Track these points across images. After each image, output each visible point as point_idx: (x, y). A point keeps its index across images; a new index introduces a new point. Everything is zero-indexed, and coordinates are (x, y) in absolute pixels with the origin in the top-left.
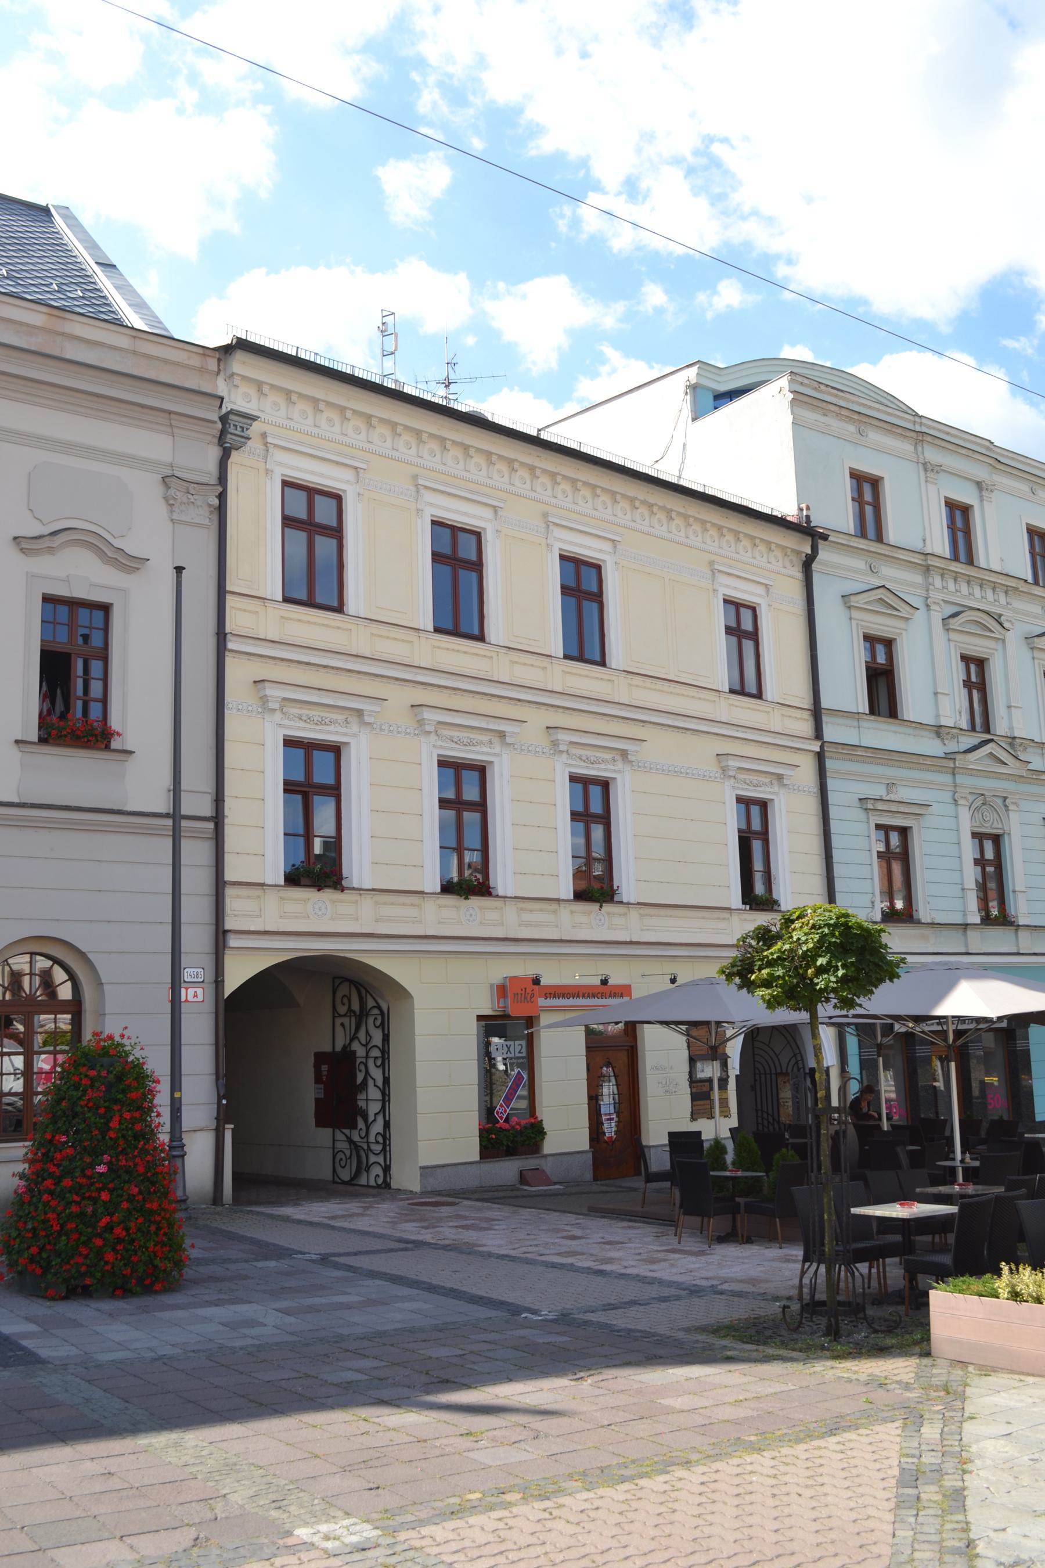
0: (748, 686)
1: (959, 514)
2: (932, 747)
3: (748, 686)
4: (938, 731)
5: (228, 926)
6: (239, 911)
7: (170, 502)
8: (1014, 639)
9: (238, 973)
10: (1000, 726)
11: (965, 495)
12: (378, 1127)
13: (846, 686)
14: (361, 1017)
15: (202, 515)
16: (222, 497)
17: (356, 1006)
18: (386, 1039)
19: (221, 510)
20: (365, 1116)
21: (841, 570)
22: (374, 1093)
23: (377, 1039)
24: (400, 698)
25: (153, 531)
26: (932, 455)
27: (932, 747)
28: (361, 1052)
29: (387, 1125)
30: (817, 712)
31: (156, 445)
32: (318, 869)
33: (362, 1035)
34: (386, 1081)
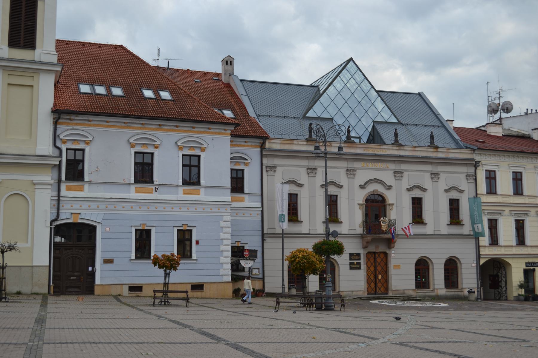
5: (481, 253)
6: (483, 251)
7: (467, 179)
9: (482, 261)
12: (505, 289)
14: (500, 268)
16: (476, 177)
17: (499, 266)
18: (506, 272)
19: (476, 180)
20: (501, 287)
22: (503, 283)
23: (504, 272)
24: (507, 210)
25: (464, 184)
28: (500, 275)
29: (506, 288)
31: (464, 169)
32: (494, 242)
33: (500, 272)
34: (506, 280)
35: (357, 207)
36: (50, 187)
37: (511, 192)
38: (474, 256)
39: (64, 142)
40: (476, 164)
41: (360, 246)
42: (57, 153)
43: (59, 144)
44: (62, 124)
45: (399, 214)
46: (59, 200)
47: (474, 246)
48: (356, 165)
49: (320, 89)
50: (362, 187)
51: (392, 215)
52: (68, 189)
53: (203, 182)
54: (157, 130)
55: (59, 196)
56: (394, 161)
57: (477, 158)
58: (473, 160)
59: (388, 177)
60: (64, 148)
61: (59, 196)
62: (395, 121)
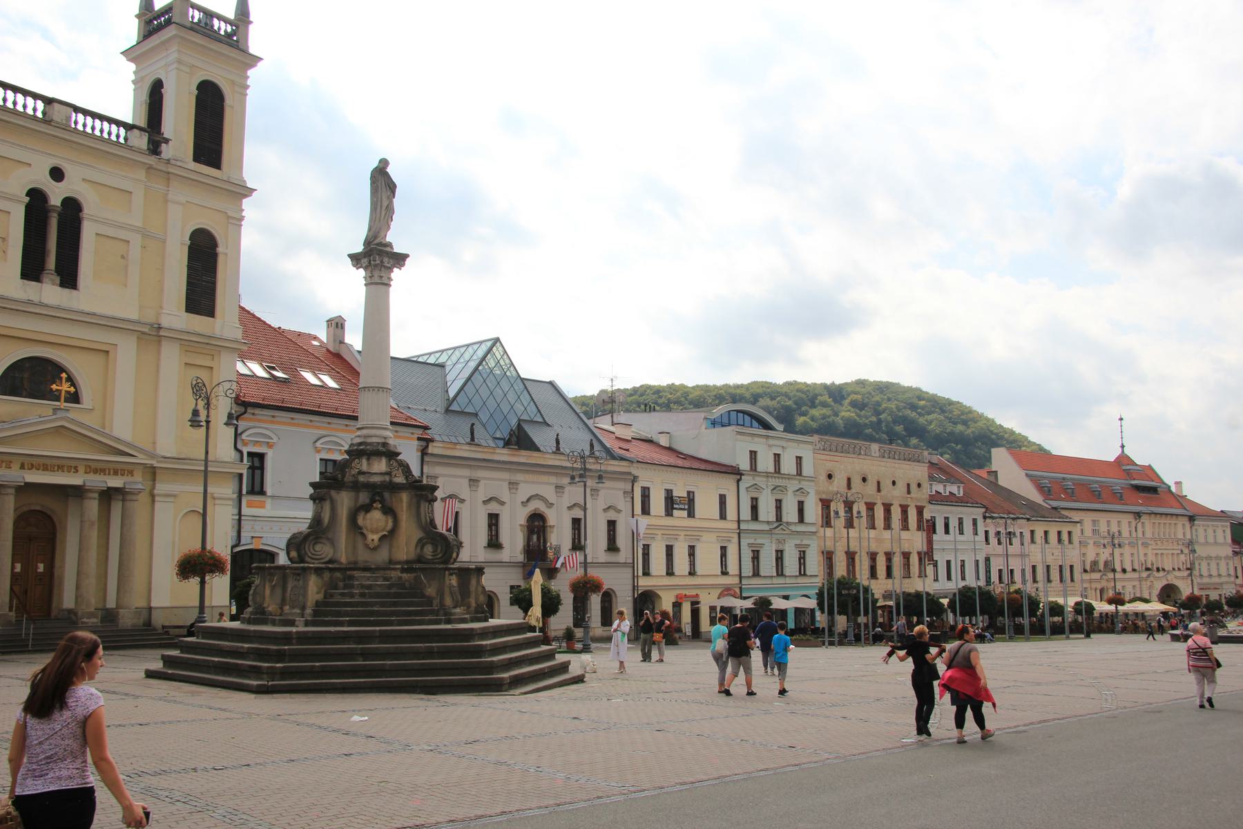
0: (723, 516)
1: (777, 456)
2: (766, 527)
3: (723, 516)
4: (768, 522)
8: (790, 493)
10: (784, 520)
13: (746, 513)
15: (629, 499)
21: (747, 481)
24: (659, 532)
25: (623, 504)
26: (771, 442)
27: (766, 527)
30: (739, 521)
35: (519, 528)
36: (230, 502)
37: (718, 517)
38: (631, 587)
39: (245, 444)
40: (634, 479)
41: (521, 576)
42: (238, 455)
43: (239, 446)
44: (246, 419)
45: (559, 537)
46: (240, 520)
47: (630, 576)
48: (519, 477)
49: (450, 378)
50: (525, 504)
51: (553, 539)
52: (250, 505)
53: (269, 489)
54: (343, 431)
55: (240, 514)
56: (556, 474)
57: (635, 472)
58: (629, 473)
59: (549, 492)
60: (245, 450)
61: (240, 514)
62: (540, 420)
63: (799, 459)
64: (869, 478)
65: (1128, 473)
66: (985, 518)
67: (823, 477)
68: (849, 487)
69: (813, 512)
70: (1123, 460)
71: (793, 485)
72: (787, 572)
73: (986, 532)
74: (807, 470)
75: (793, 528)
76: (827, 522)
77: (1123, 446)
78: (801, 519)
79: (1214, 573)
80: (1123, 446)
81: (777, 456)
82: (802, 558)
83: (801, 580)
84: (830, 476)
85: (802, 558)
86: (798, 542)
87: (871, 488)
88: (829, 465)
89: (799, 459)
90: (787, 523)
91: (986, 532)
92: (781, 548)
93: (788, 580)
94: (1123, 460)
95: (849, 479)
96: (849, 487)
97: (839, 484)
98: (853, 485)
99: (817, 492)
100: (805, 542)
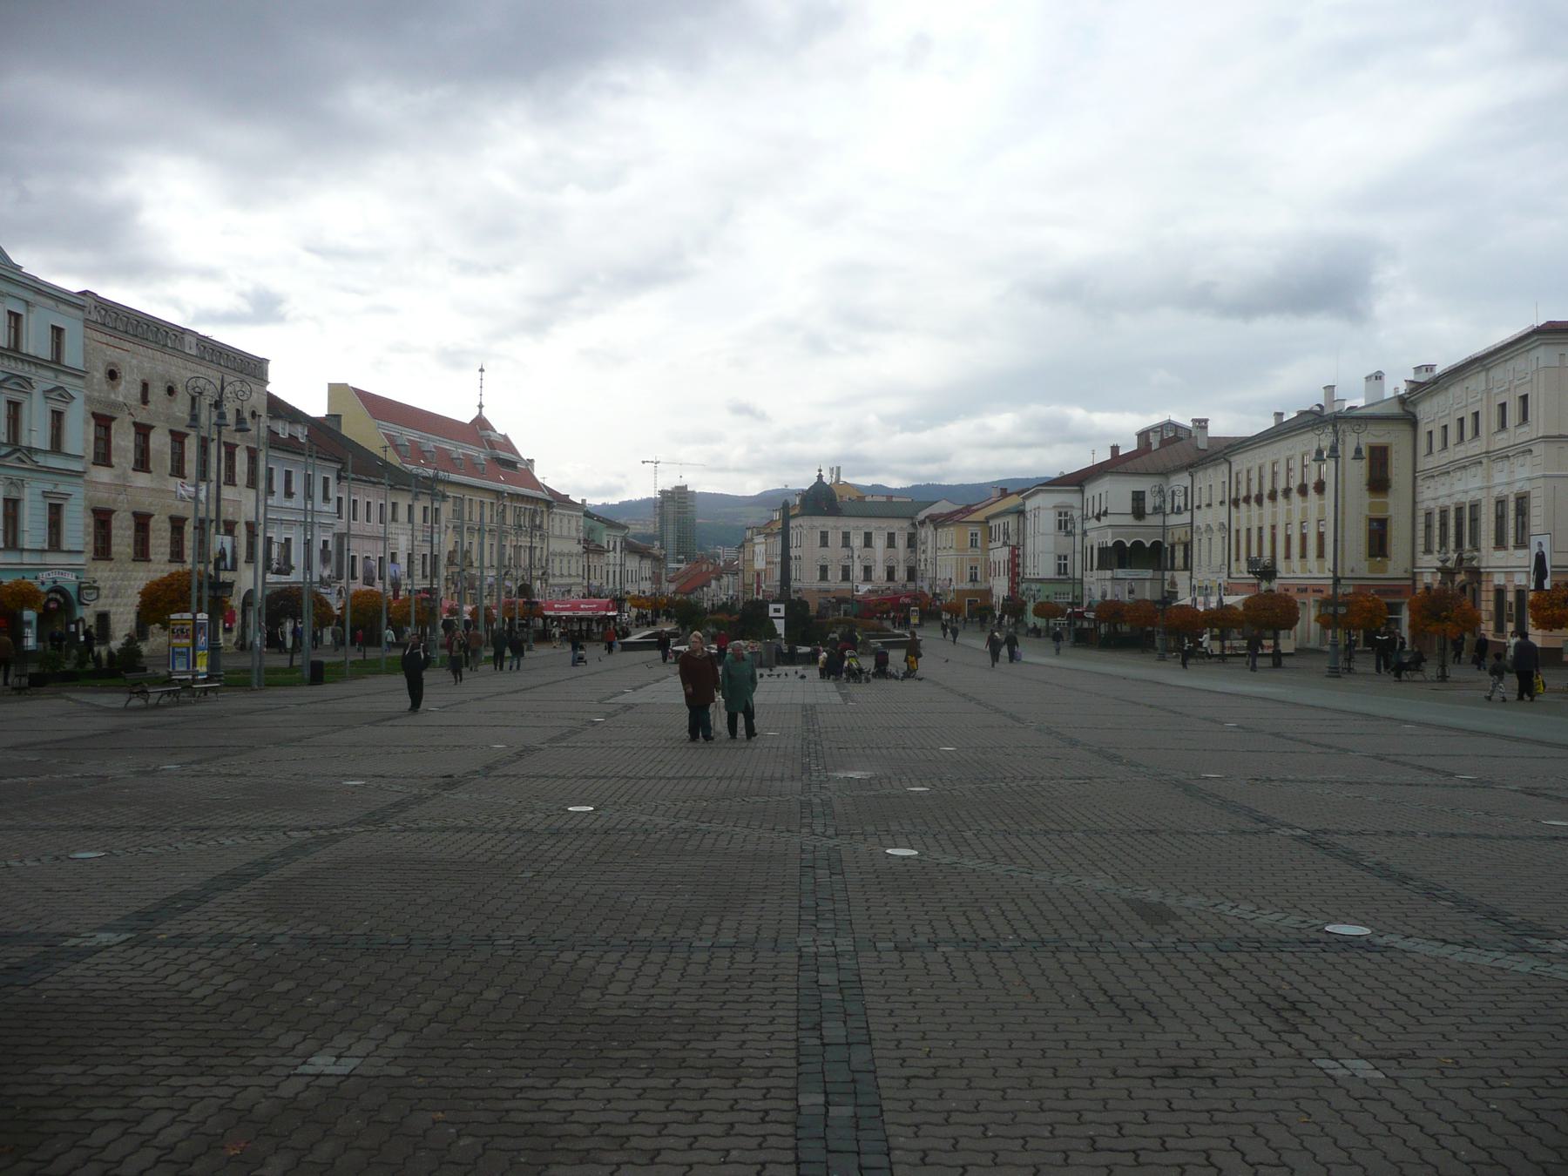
8: (37, 394)
10: (24, 442)
11: (19, 308)
63: (58, 332)
64: (179, 388)
65: (492, 444)
66: (339, 478)
67: (99, 375)
68: (145, 401)
69: (79, 435)
70: (480, 423)
71: (44, 380)
72: (27, 541)
73: (340, 499)
74: (73, 355)
75: (42, 460)
76: (103, 457)
77: (481, 406)
78: (56, 446)
79: (565, 572)
80: (481, 406)
81: (15, 317)
82: (55, 512)
83: (51, 558)
84: (113, 375)
85: (55, 512)
86: (48, 487)
87: (181, 408)
88: (113, 355)
89: (58, 332)
90: (30, 449)
91: (340, 499)
92: (14, 495)
93: (27, 558)
94: (480, 423)
95: (145, 386)
96: (145, 401)
97: (127, 391)
98: (151, 397)
99: (89, 400)
100: (62, 489)
